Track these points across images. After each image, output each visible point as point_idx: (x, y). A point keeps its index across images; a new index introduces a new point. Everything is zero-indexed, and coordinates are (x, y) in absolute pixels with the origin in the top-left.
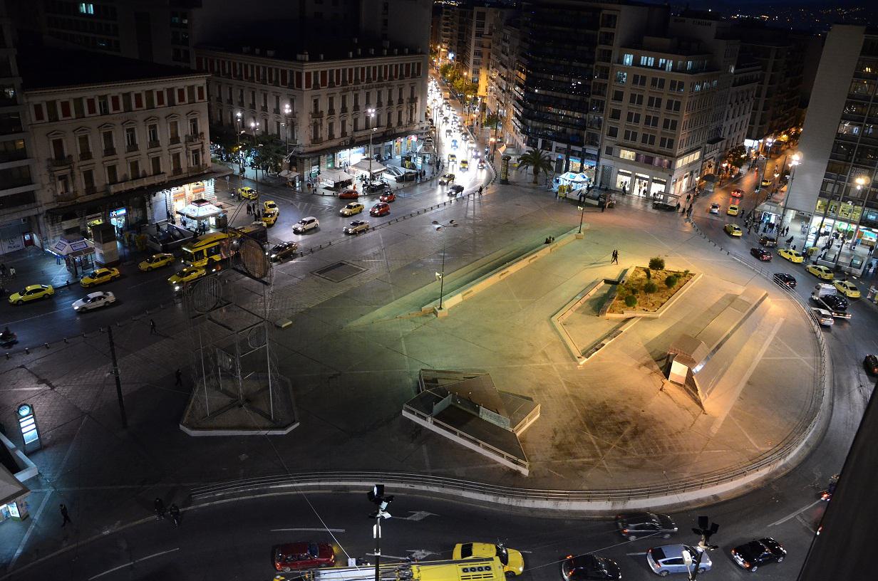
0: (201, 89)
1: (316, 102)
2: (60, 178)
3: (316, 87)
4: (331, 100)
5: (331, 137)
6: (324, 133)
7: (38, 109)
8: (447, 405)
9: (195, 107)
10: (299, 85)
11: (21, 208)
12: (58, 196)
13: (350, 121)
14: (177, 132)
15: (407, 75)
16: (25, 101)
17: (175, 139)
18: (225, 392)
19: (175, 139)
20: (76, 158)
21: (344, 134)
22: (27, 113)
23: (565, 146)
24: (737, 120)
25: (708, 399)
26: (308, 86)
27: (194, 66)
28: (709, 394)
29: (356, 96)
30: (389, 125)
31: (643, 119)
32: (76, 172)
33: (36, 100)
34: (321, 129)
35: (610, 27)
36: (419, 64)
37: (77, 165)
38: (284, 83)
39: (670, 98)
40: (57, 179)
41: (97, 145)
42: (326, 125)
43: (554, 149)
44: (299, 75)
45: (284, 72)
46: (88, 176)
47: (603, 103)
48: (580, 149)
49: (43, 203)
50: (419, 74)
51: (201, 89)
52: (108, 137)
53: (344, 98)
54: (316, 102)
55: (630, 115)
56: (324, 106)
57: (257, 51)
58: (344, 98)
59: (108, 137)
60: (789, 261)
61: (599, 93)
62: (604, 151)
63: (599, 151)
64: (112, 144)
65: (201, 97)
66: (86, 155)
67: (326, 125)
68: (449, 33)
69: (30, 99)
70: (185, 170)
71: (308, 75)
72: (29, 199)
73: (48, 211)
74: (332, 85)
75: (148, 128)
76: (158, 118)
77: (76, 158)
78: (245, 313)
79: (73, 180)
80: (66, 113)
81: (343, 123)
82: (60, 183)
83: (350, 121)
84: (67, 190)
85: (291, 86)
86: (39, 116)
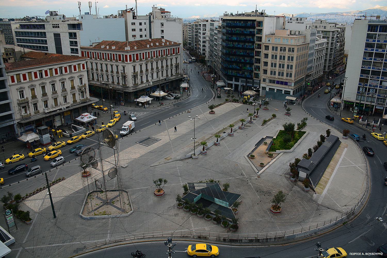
0: (83, 65)
1: (134, 67)
2: (23, 107)
3: (134, 61)
4: (141, 66)
5: (142, 82)
6: (139, 81)
7: (12, 78)
8: (200, 198)
9: (82, 73)
10: (127, 61)
11: (6, 121)
12: (22, 115)
13: (150, 75)
14: (73, 84)
15: (174, 53)
16: (7, 74)
17: (73, 88)
18: (101, 199)
19: (73, 88)
20: (30, 99)
21: (147, 81)
22: (8, 81)
23: (245, 80)
24: (319, 63)
25: (317, 187)
26: (130, 60)
27: (80, 55)
28: (317, 185)
29: (152, 64)
30: (167, 75)
31: (278, 65)
32: (30, 104)
33: (12, 74)
34: (137, 79)
35: (260, 27)
36: (179, 48)
37: (30, 102)
38: (120, 60)
39: (289, 55)
40: (22, 108)
41: (38, 92)
42: (139, 77)
43: (240, 81)
44: (126, 56)
45: (120, 55)
46: (35, 105)
47: (260, 59)
48: (252, 81)
49: (16, 118)
50: (179, 52)
51: (83, 65)
52: (43, 88)
53: (146, 65)
54: (134, 67)
55: (272, 64)
56: (138, 69)
57: (108, 47)
58: (146, 65)
59: (43, 88)
60: (347, 122)
61: (258, 56)
62: (262, 80)
63: (260, 80)
64: (45, 91)
65: (84, 68)
66: (34, 97)
67: (139, 77)
68: (191, 34)
69: (9, 74)
70: (78, 101)
71: (130, 56)
72: (10, 117)
73: (18, 122)
74: (141, 60)
75: (61, 83)
76: (65, 79)
77: (30, 99)
78: (107, 163)
79: (29, 108)
80: (25, 78)
81: (147, 75)
82: (23, 110)
83: (150, 75)
84: (26, 113)
85: (123, 61)
86: (13, 81)
